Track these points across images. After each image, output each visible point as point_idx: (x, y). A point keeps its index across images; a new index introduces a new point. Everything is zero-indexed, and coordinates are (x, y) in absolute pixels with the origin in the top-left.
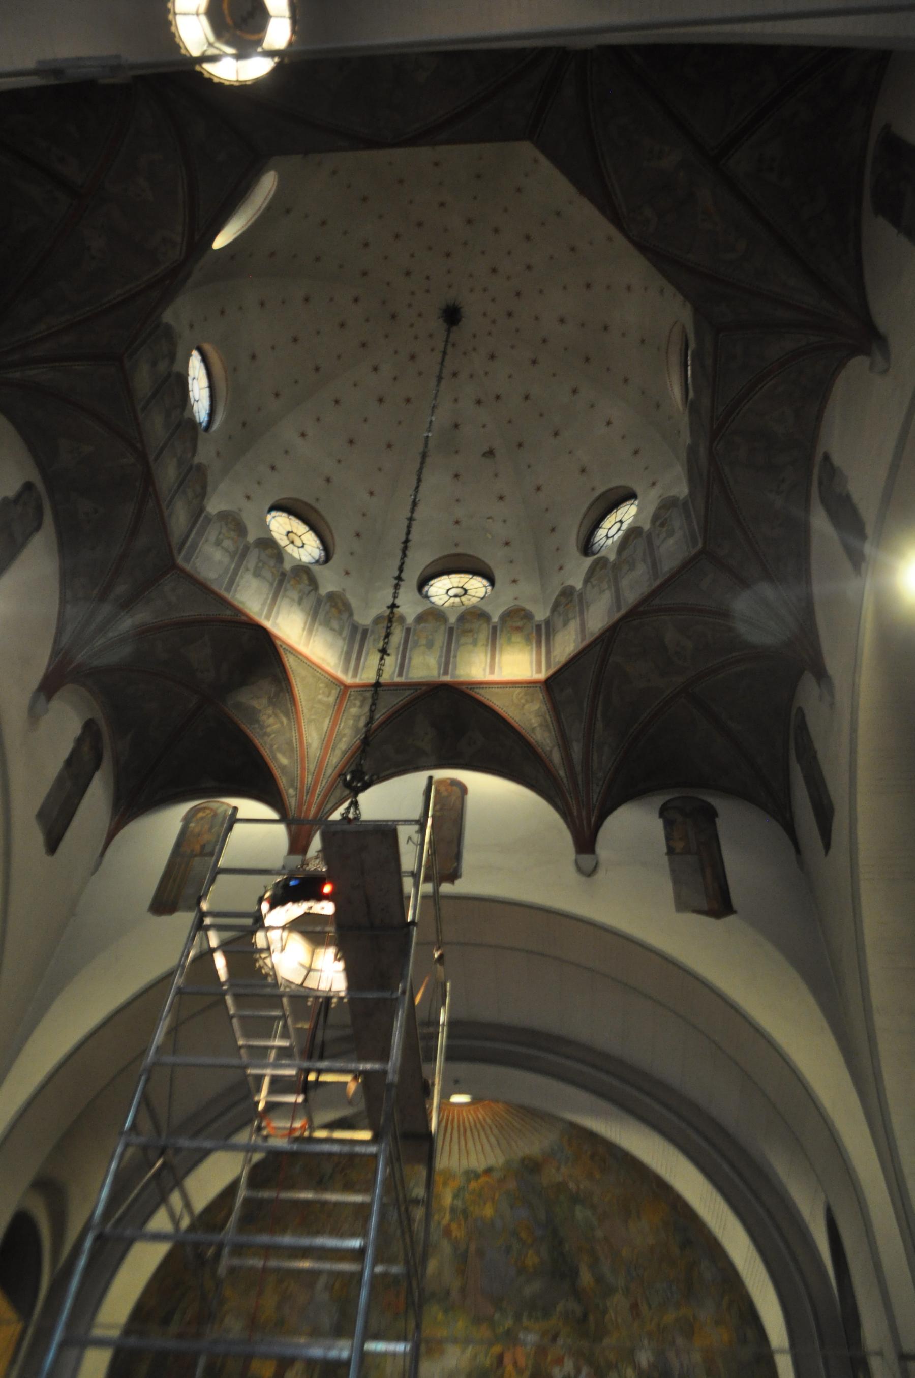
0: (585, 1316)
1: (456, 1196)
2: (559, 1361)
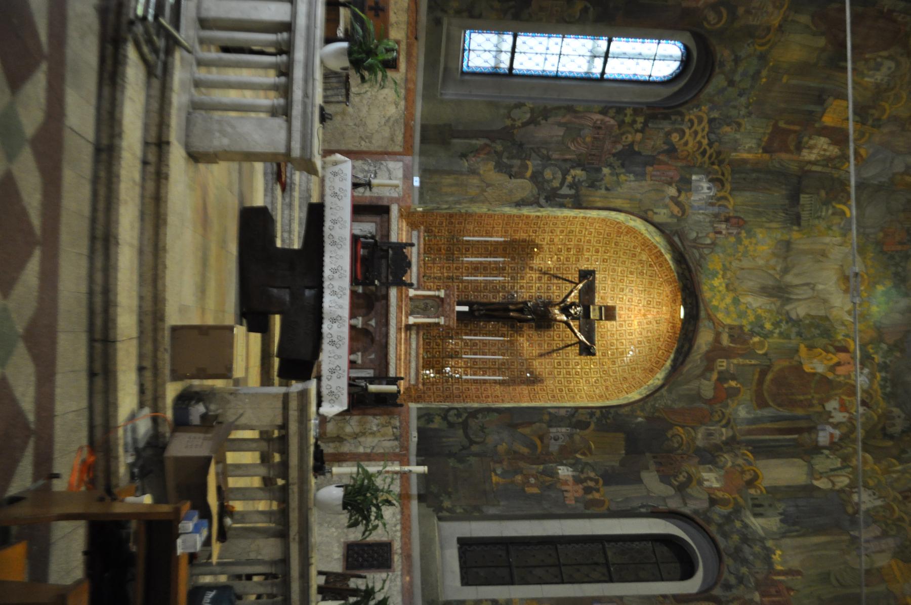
0: (891, 437)
2: (843, 407)
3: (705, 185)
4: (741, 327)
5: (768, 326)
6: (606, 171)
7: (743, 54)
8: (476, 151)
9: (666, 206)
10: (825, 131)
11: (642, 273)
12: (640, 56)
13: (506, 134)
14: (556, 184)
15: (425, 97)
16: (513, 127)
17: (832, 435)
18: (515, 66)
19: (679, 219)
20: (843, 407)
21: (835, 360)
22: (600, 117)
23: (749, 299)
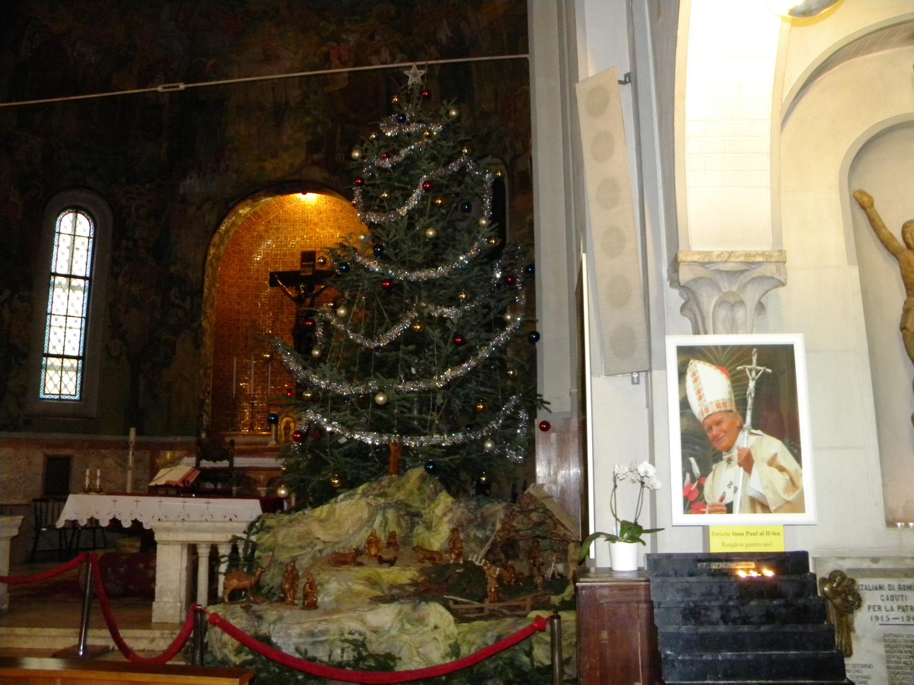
3: (188, 182)
4: (308, 143)
5: (308, 120)
6: (172, 269)
11: (277, 229)
12: (72, 248)
18: (76, 354)
22: (120, 278)
23: (285, 137)
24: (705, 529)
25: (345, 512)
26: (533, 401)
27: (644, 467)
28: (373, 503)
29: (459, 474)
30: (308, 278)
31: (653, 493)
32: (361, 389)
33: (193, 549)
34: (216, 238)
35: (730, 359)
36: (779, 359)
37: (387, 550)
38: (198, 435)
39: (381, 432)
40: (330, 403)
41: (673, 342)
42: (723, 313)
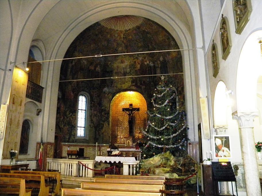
1: (124, 35)
3: (105, 89)
4: (132, 81)
6: (102, 108)
7: (81, 86)
8: (99, 133)
9: (109, 96)
10: (95, 69)
13: (96, 128)
14: (105, 118)
15: (89, 143)
16: (94, 126)
17: (151, 63)
19: (111, 94)
20: (146, 61)
21: (137, 63)
22: (92, 111)
24: (218, 159)
25: (156, 159)
26: (187, 139)
27: (211, 152)
28: (161, 157)
29: (174, 152)
30: (131, 110)
31: (211, 155)
32: (158, 138)
33: (129, 166)
34: (112, 101)
35: (221, 138)
36: (227, 138)
37: (164, 165)
38: (109, 144)
39: (162, 145)
40: (153, 140)
41: (214, 135)
42: (220, 132)
